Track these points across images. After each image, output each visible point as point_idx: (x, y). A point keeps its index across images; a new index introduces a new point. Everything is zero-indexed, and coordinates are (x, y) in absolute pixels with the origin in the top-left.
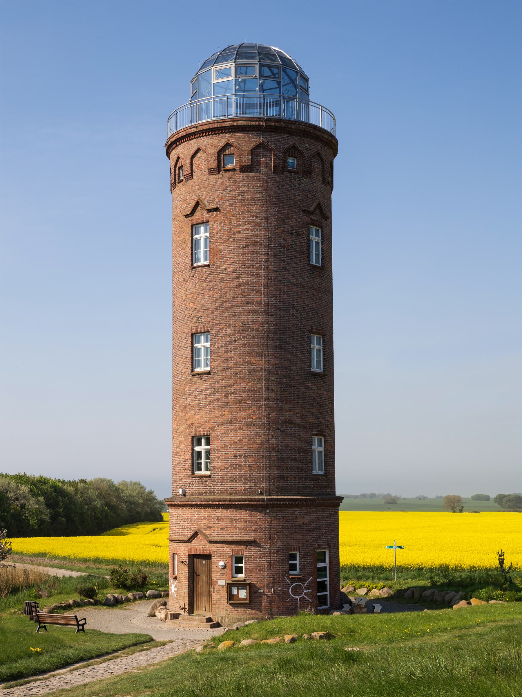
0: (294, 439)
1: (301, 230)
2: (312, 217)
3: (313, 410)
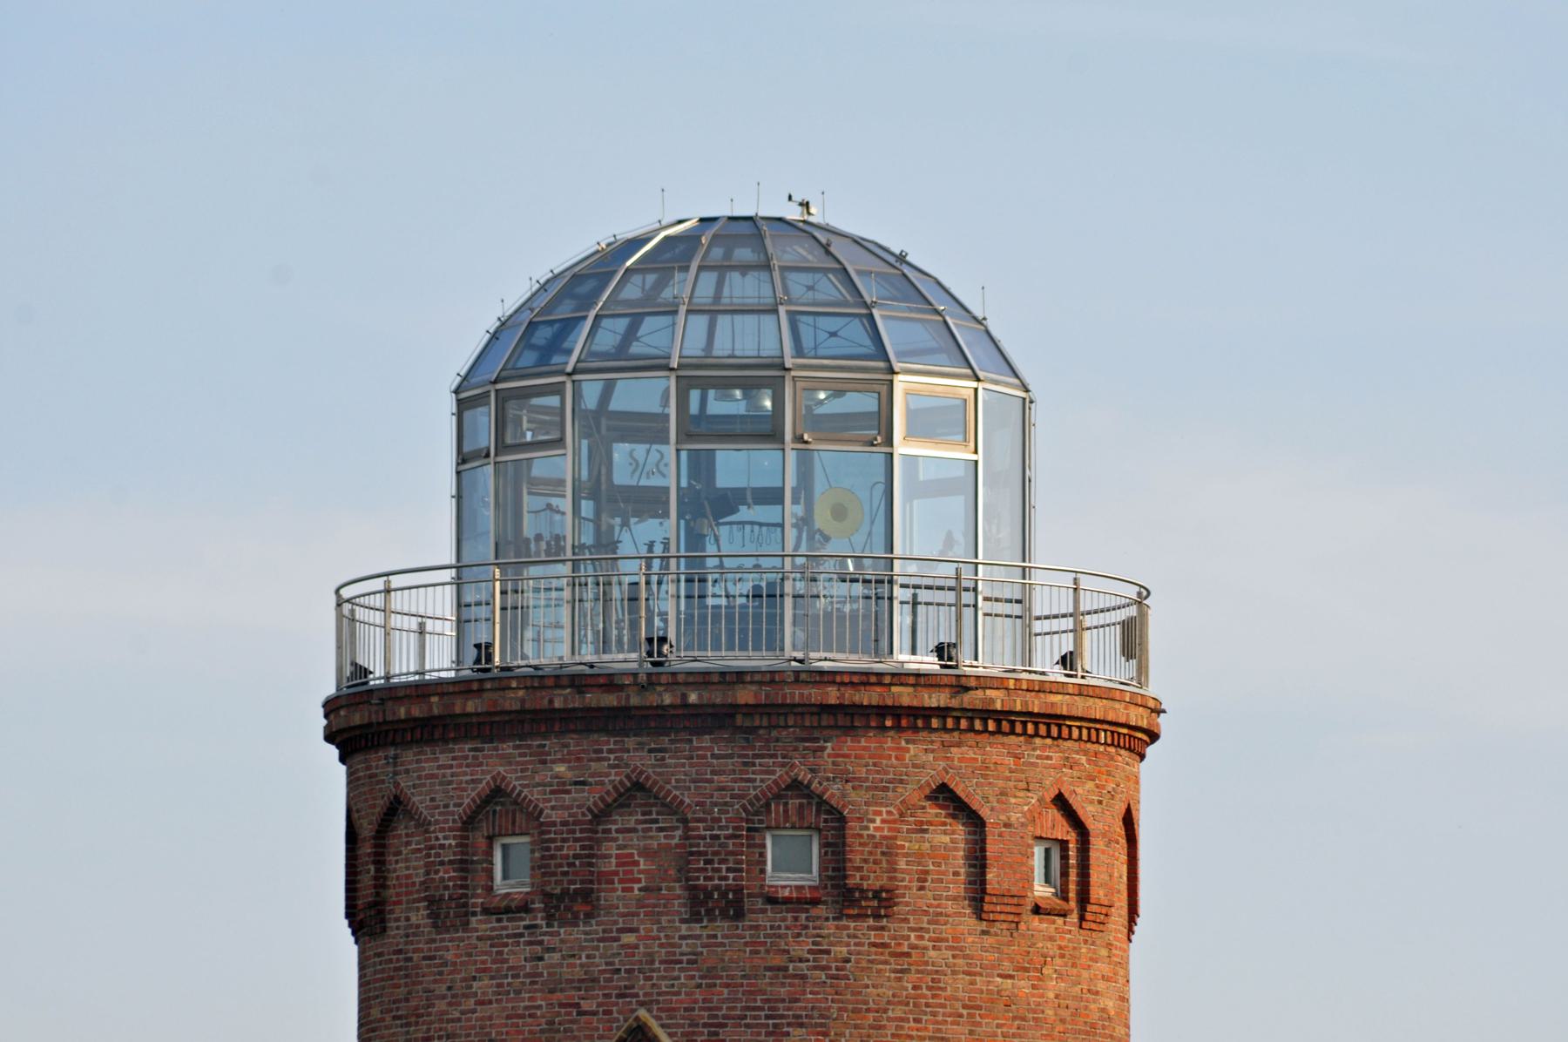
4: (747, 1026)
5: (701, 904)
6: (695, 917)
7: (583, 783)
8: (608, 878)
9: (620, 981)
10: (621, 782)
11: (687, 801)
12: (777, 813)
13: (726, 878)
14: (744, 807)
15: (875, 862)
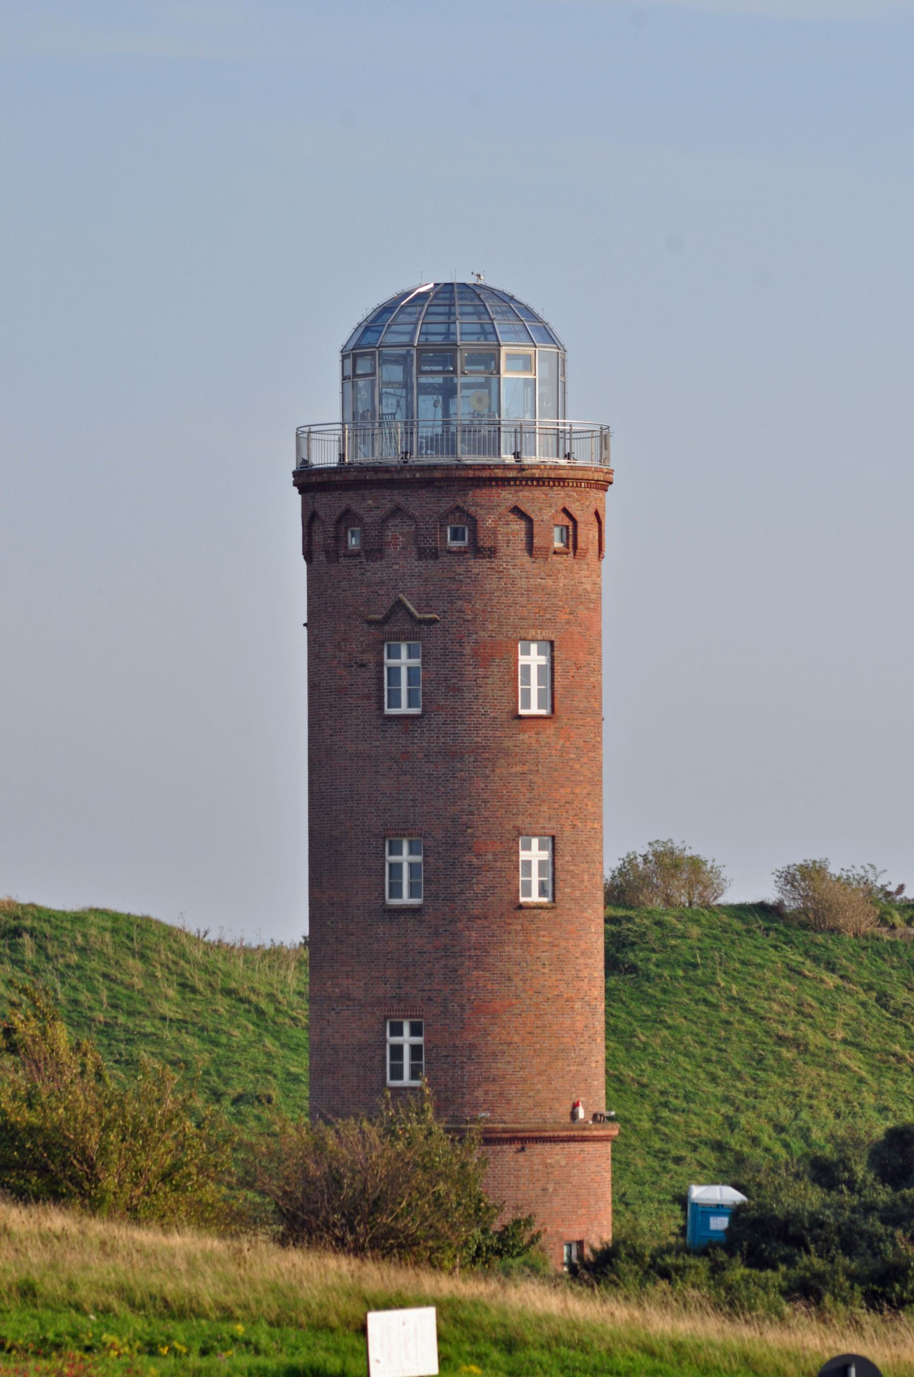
0: (353, 1026)
1: (365, 656)
2: (387, 628)
5: (422, 554)
6: (420, 559)
8: (388, 543)
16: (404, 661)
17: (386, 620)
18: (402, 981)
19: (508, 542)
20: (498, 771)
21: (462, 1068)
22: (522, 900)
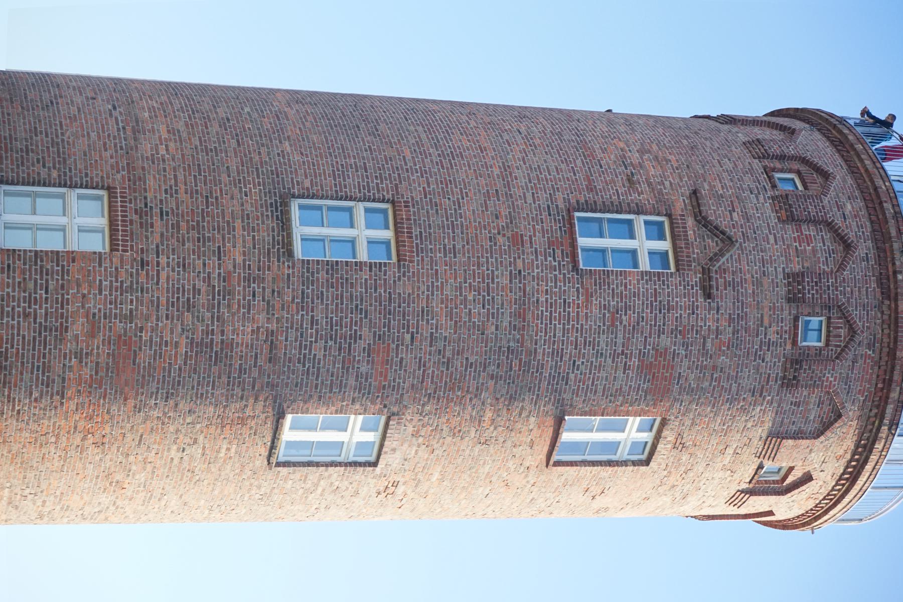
0: (93, 135)
1: (644, 186)
2: (690, 222)
3: (182, 196)
4: (734, 303)
5: (795, 278)
7: (845, 218)
8: (799, 230)
9: (750, 232)
10: (849, 238)
11: (845, 273)
12: (838, 323)
13: (809, 293)
14: (843, 304)
15: (812, 377)
16: (645, 245)
17: (703, 221)
18: (172, 220)
19: (797, 404)
20: (491, 383)
21: (26, 315)
22: (289, 418)
